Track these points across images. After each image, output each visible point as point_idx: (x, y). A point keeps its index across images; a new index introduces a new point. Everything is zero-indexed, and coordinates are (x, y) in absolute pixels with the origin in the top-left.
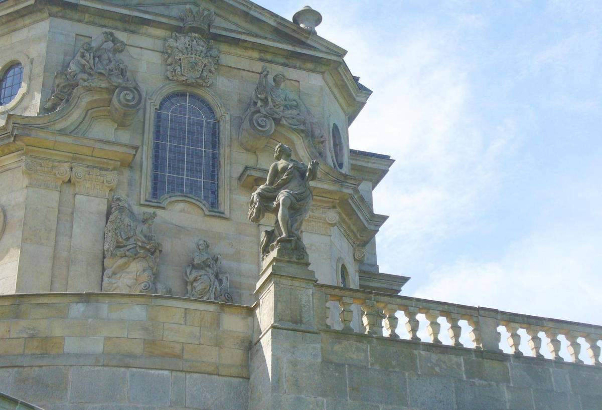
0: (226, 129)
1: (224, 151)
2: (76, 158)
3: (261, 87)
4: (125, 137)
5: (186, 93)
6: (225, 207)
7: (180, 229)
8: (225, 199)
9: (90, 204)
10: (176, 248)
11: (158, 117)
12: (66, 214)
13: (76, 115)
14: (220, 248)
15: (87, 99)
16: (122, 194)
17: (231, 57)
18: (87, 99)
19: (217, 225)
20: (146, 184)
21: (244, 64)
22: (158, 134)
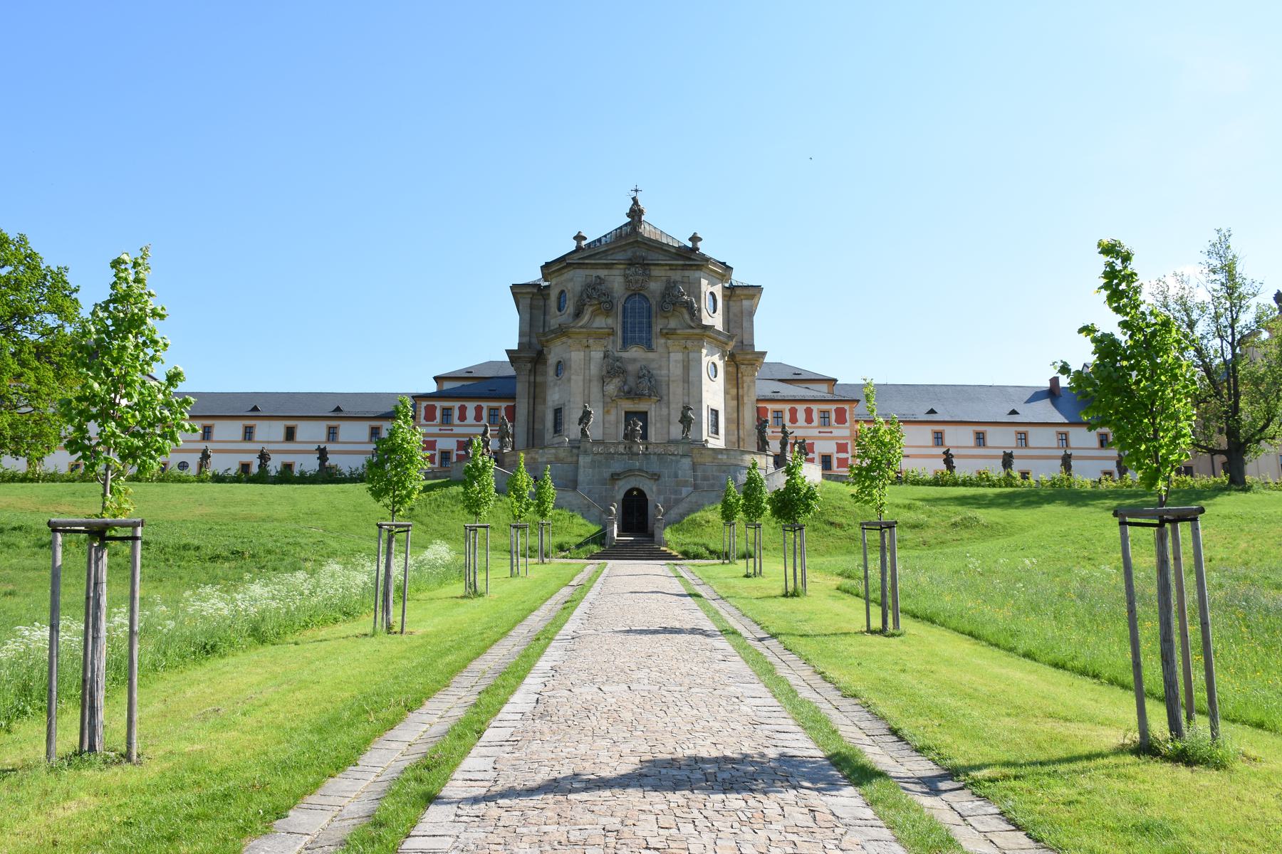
0: (654, 307)
1: (654, 320)
2: (589, 335)
3: (667, 288)
4: (610, 321)
5: (636, 294)
6: (654, 347)
7: (634, 360)
8: (654, 341)
9: (597, 355)
11: (624, 309)
12: (588, 360)
13: (586, 318)
14: (653, 365)
15: (591, 309)
16: (610, 347)
17: (656, 272)
18: (591, 309)
19: (651, 355)
20: (620, 342)
21: (663, 273)
22: (624, 316)
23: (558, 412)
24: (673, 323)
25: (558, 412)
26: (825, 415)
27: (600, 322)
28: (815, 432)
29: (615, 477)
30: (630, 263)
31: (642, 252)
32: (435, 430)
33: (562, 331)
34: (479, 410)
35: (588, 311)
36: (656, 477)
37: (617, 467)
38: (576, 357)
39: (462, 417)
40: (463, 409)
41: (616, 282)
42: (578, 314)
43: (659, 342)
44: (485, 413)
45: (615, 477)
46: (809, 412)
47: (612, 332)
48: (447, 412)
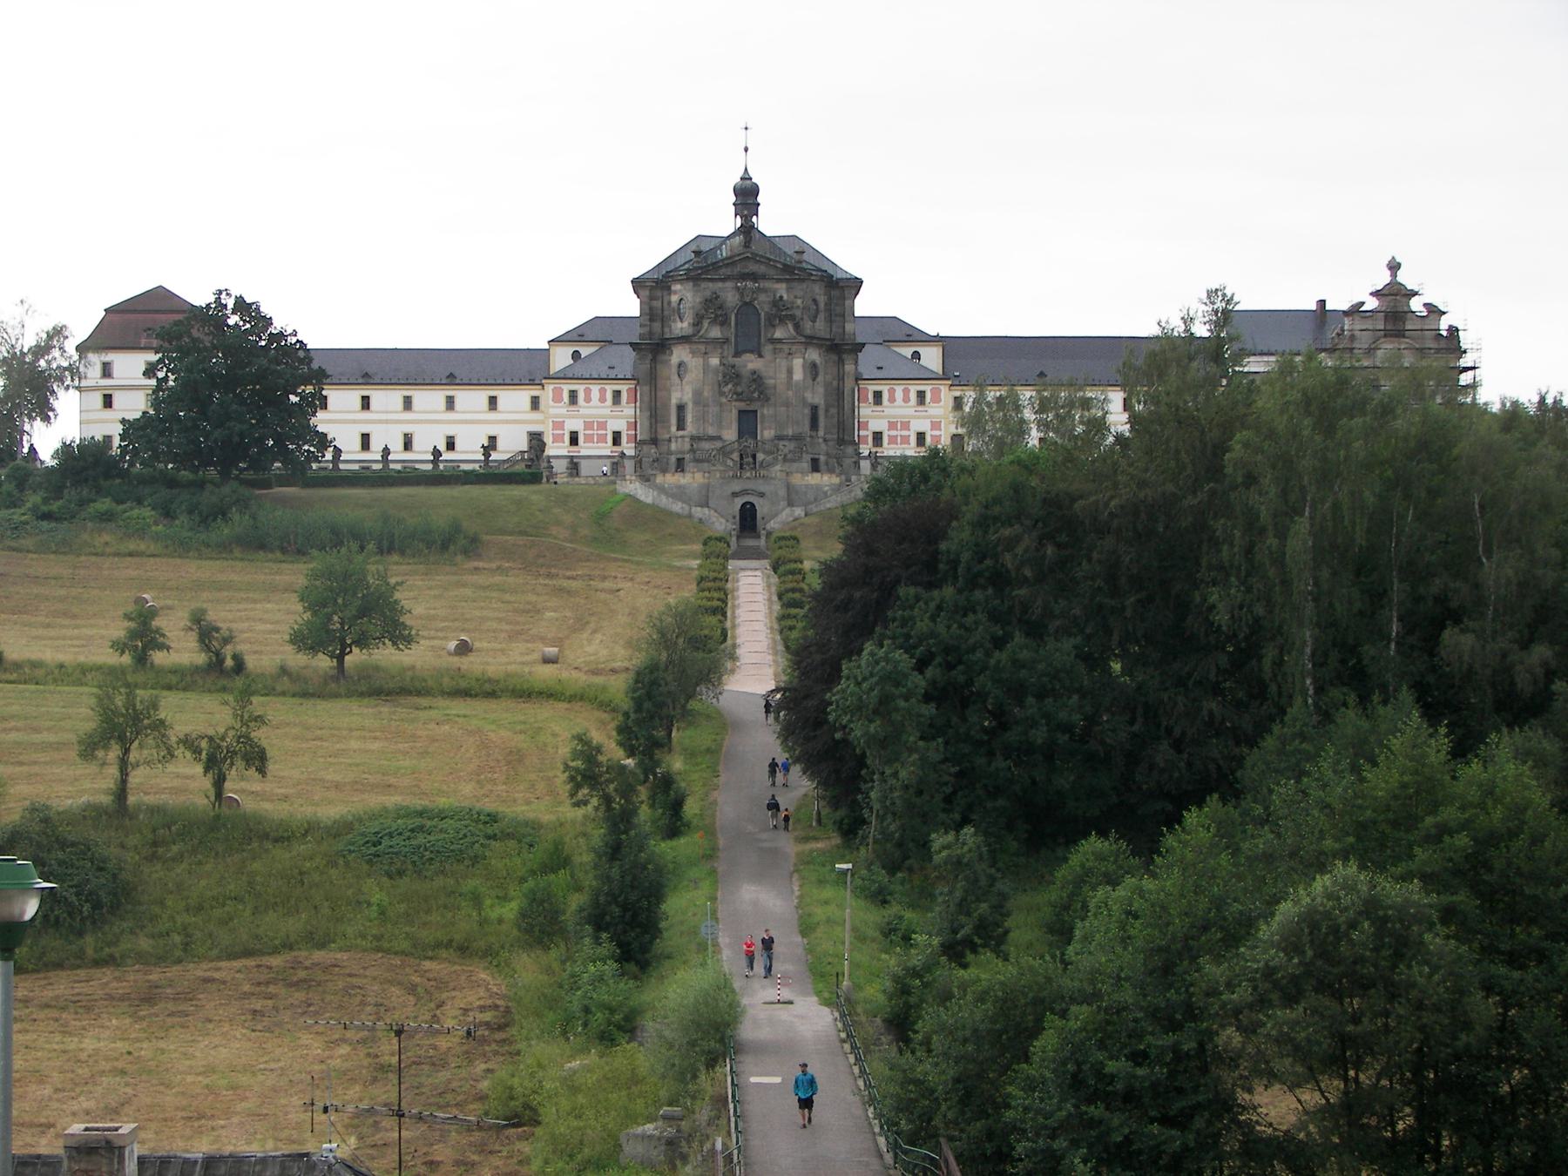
5: (747, 307)
9: (715, 361)
10: (745, 372)
23: (681, 408)
24: (778, 334)
25: (681, 408)
26: (921, 395)
27: (716, 332)
28: (911, 411)
29: (735, 495)
30: (744, 277)
31: (753, 267)
32: (564, 411)
33: (684, 339)
34: (603, 392)
35: (706, 324)
36: (762, 495)
37: (737, 488)
38: (694, 363)
39: (588, 399)
40: (588, 391)
41: (730, 297)
42: (697, 324)
43: (767, 349)
44: (609, 396)
45: (735, 495)
46: (906, 392)
47: (726, 341)
48: (573, 396)
